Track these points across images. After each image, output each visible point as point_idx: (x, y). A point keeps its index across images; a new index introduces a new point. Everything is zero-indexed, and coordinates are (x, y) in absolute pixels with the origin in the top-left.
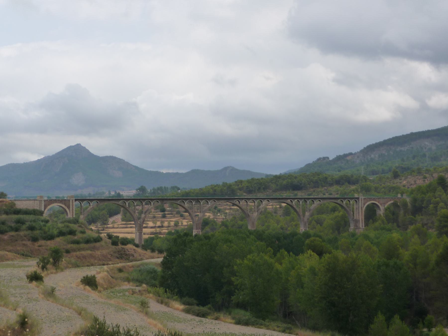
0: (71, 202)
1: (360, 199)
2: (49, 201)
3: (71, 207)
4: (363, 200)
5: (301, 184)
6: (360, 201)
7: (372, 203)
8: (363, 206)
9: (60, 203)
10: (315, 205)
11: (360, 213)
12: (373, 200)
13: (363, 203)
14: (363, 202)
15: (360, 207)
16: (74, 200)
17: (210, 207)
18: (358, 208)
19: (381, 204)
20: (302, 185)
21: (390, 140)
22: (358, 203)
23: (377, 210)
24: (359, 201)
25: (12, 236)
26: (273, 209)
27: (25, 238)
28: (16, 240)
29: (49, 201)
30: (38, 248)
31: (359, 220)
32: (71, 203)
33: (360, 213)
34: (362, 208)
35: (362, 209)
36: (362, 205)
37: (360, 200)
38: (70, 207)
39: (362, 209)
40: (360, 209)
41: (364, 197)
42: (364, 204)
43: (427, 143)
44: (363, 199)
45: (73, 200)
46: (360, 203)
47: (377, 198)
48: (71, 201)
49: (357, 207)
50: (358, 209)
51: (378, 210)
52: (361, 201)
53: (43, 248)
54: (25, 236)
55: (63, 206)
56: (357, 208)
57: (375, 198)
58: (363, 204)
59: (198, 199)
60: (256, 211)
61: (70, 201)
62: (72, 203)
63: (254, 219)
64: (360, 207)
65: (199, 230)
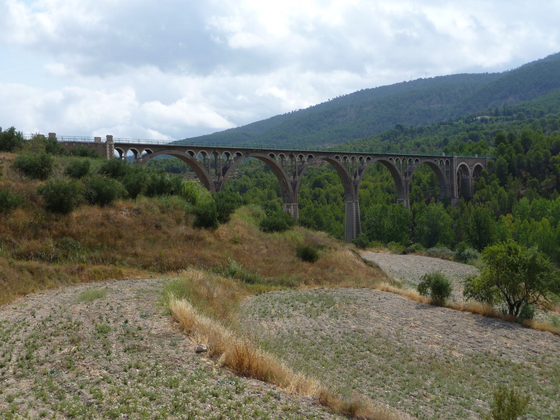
0: (108, 149)
2: (66, 144)
7: (460, 167)
16: (113, 146)
19: (469, 166)
22: (450, 164)
35: (456, 173)
36: (455, 168)
39: (456, 173)
42: (457, 166)
48: (108, 146)
49: (449, 170)
50: (451, 173)
52: (455, 162)
56: (447, 171)
59: (292, 151)
60: (358, 174)
61: (106, 147)
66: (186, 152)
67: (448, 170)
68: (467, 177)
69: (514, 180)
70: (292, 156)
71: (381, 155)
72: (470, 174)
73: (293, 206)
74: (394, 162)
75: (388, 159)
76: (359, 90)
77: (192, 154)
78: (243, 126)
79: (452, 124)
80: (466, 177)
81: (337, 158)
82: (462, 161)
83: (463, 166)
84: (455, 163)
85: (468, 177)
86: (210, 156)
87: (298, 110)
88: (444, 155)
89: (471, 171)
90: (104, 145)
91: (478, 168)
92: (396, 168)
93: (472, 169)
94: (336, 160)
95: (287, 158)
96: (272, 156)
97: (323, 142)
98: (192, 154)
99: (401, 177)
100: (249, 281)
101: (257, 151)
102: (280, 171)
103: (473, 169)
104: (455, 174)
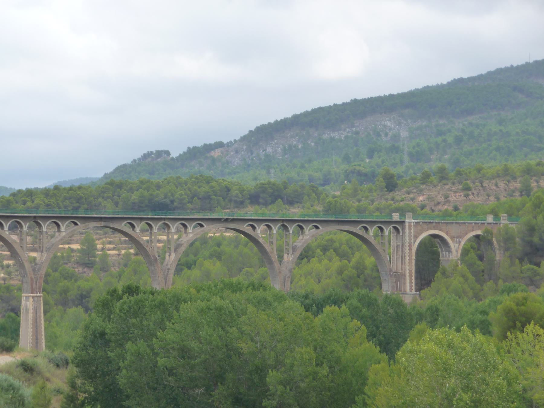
1: (407, 224)
4: (412, 227)
5: (172, 202)
6: (407, 231)
8: (412, 241)
10: (306, 237)
12: (435, 228)
13: (412, 234)
14: (412, 231)
15: (407, 245)
17: (64, 237)
18: (401, 246)
19: (452, 238)
20: (176, 204)
21: (306, 114)
22: (401, 234)
23: (442, 251)
24: (403, 229)
26: (121, 257)
31: (404, 275)
36: (410, 239)
37: (407, 227)
41: (416, 221)
42: (416, 237)
43: (389, 124)
44: (412, 224)
47: (444, 223)
50: (402, 249)
51: (444, 253)
52: (410, 229)
56: (397, 246)
57: (439, 223)
58: (412, 238)
60: (173, 249)
63: (169, 269)
64: (407, 245)
65: (38, 294)
67: (399, 244)
68: (449, 257)
72: (454, 251)
73: (33, 297)
80: (448, 256)
82: (431, 229)
84: (410, 233)
85: (451, 256)
93: (460, 242)
103: (463, 243)
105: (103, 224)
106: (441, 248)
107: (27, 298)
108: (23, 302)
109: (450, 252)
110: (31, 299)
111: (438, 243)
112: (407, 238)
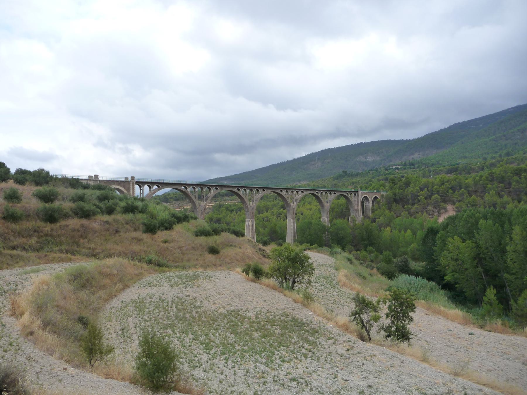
0: (131, 185)
2: (105, 182)
3: (131, 190)
6: (359, 195)
7: (363, 197)
9: (118, 185)
11: (360, 204)
15: (359, 200)
16: (135, 183)
19: (370, 197)
25: (107, 222)
27: (128, 227)
28: (117, 232)
29: (105, 182)
30: (165, 245)
32: (131, 186)
33: (360, 204)
34: (360, 200)
38: (130, 191)
40: (359, 201)
45: (133, 182)
46: (359, 196)
48: (131, 183)
53: (172, 244)
54: (127, 224)
55: (122, 189)
59: (251, 187)
60: (295, 201)
61: (130, 184)
62: (132, 185)
64: (359, 200)
66: (183, 187)
69: (396, 206)
70: (251, 190)
71: (311, 190)
74: (319, 195)
75: (315, 193)
76: (324, 149)
77: (186, 188)
78: (252, 171)
79: (376, 171)
81: (282, 191)
83: (365, 197)
86: (198, 189)
87: (286, 161)
88: (353, 190)
89: (371, 200)
90: (129, 182)
91: (376, 198)
92: (321, 198)
93: (371, 199)
94: (281, 193)
95: (248, 191)
96: (239, 190)
97: (300, 180)
98: (186, 188)
99: (324, 203)
100: (159, 265)
101: (228, 186)
102: (244, 200)
104: (359, 202)
105: (273, 191)
106: (365, 201)
107: (248, 221)
108: (246, 222)
109: (369, 202)
110: (251, 221)
111: (364, 199)
112: (359, 197)
